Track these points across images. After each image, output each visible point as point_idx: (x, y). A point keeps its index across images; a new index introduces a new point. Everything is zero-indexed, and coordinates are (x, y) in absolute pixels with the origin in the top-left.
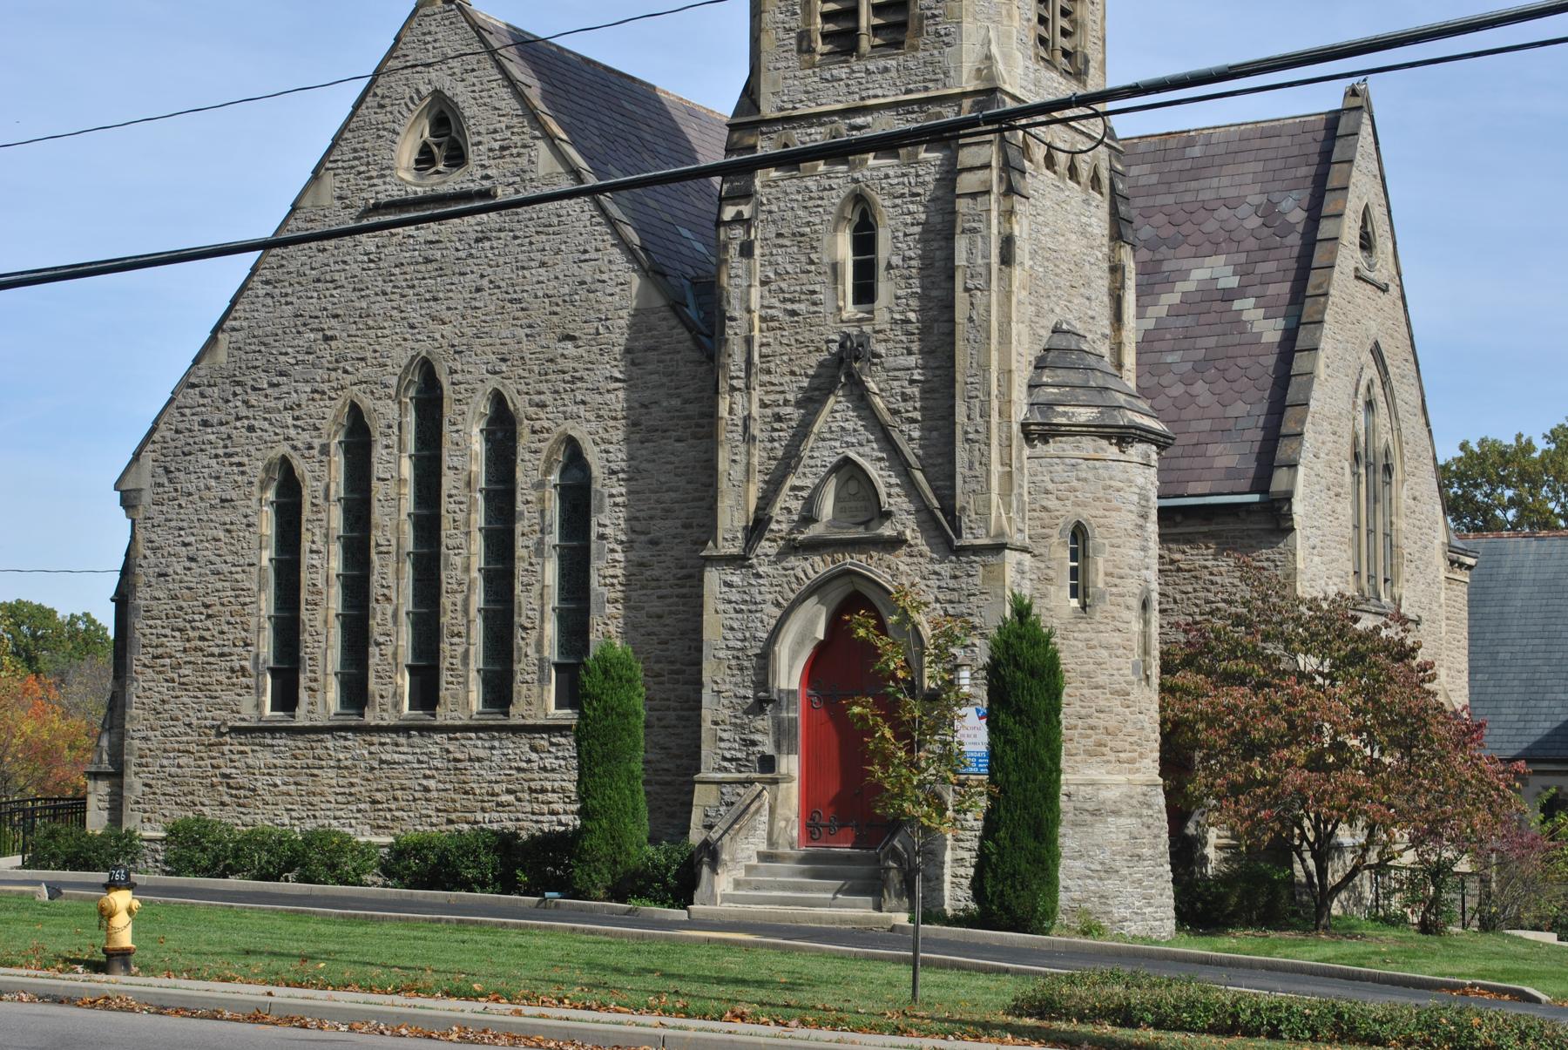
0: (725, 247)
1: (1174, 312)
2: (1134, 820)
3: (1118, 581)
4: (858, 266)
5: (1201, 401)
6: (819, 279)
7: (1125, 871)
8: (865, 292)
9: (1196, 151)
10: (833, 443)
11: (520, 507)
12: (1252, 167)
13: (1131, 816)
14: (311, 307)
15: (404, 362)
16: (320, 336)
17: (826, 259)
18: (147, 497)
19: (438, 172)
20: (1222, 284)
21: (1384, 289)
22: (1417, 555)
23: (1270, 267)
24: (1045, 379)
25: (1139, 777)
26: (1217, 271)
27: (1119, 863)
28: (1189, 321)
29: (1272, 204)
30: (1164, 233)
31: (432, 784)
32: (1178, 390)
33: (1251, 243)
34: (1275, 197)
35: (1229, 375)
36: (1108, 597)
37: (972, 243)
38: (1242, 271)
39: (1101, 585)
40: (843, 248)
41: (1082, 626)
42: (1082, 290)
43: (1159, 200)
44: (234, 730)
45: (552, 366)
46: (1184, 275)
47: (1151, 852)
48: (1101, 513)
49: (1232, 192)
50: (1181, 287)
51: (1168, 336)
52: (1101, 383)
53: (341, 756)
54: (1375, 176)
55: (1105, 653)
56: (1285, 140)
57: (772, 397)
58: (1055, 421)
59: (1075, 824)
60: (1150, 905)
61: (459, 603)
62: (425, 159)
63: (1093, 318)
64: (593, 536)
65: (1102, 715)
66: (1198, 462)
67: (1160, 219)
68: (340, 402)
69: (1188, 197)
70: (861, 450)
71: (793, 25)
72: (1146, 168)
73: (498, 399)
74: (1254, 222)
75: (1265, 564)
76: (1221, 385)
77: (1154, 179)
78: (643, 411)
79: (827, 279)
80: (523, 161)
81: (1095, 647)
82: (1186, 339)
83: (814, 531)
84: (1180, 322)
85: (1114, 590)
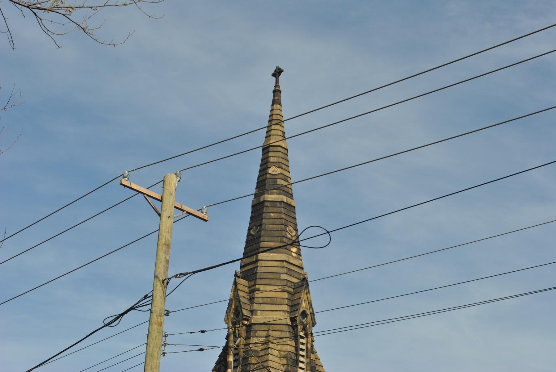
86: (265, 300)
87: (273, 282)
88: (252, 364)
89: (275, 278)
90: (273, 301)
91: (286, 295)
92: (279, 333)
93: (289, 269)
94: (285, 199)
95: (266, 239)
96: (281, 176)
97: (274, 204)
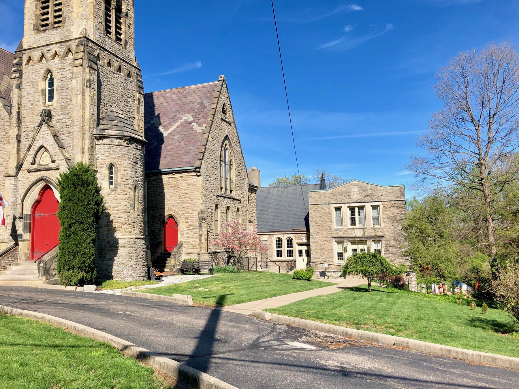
1: (178, 127)
2: (129, 249)
4: (50, 91)
6: (39, 94)
7: (127, 263)
8: (51, 98)
9: (187, 91)
10: (39, 141)
17: (40, 89)
20: (189, 120)
21: (230, 124)
23: (201, 116)
24: (104, 123)
25: (134, 236)
26: (189, 117)
27: (124, 261)
28: (181, 128)
29: (202, 102)
33: (197, 111)
35: (189, 140)
36: (122, 185)
38: (194, 117)
39: (119, 181)
40: (44, 85)
41: (112, 193)
42: (124, 103)
43: (177, 102)
46: (181, 118)
47: (136, 257)
48: (120, 160)
49: (194, 100)
50: (180, 121)
54: (227, 98)
55: (121, 201)
56: (206, 88)
57: (25, 129)
58: (104, 134)
59: (109, 250)
60: (134, 273)
63: (129, 112)
65: (120, 219)
67: (177, 106)
69: (184, 101)
70: (47, 143)
71: (32, 22)
72: (175, 95)
74: (198, 106)
77: (177, 98)
79: (40, 94)
81: (117, 199)
83: (35, 167)
84: (179, 129)
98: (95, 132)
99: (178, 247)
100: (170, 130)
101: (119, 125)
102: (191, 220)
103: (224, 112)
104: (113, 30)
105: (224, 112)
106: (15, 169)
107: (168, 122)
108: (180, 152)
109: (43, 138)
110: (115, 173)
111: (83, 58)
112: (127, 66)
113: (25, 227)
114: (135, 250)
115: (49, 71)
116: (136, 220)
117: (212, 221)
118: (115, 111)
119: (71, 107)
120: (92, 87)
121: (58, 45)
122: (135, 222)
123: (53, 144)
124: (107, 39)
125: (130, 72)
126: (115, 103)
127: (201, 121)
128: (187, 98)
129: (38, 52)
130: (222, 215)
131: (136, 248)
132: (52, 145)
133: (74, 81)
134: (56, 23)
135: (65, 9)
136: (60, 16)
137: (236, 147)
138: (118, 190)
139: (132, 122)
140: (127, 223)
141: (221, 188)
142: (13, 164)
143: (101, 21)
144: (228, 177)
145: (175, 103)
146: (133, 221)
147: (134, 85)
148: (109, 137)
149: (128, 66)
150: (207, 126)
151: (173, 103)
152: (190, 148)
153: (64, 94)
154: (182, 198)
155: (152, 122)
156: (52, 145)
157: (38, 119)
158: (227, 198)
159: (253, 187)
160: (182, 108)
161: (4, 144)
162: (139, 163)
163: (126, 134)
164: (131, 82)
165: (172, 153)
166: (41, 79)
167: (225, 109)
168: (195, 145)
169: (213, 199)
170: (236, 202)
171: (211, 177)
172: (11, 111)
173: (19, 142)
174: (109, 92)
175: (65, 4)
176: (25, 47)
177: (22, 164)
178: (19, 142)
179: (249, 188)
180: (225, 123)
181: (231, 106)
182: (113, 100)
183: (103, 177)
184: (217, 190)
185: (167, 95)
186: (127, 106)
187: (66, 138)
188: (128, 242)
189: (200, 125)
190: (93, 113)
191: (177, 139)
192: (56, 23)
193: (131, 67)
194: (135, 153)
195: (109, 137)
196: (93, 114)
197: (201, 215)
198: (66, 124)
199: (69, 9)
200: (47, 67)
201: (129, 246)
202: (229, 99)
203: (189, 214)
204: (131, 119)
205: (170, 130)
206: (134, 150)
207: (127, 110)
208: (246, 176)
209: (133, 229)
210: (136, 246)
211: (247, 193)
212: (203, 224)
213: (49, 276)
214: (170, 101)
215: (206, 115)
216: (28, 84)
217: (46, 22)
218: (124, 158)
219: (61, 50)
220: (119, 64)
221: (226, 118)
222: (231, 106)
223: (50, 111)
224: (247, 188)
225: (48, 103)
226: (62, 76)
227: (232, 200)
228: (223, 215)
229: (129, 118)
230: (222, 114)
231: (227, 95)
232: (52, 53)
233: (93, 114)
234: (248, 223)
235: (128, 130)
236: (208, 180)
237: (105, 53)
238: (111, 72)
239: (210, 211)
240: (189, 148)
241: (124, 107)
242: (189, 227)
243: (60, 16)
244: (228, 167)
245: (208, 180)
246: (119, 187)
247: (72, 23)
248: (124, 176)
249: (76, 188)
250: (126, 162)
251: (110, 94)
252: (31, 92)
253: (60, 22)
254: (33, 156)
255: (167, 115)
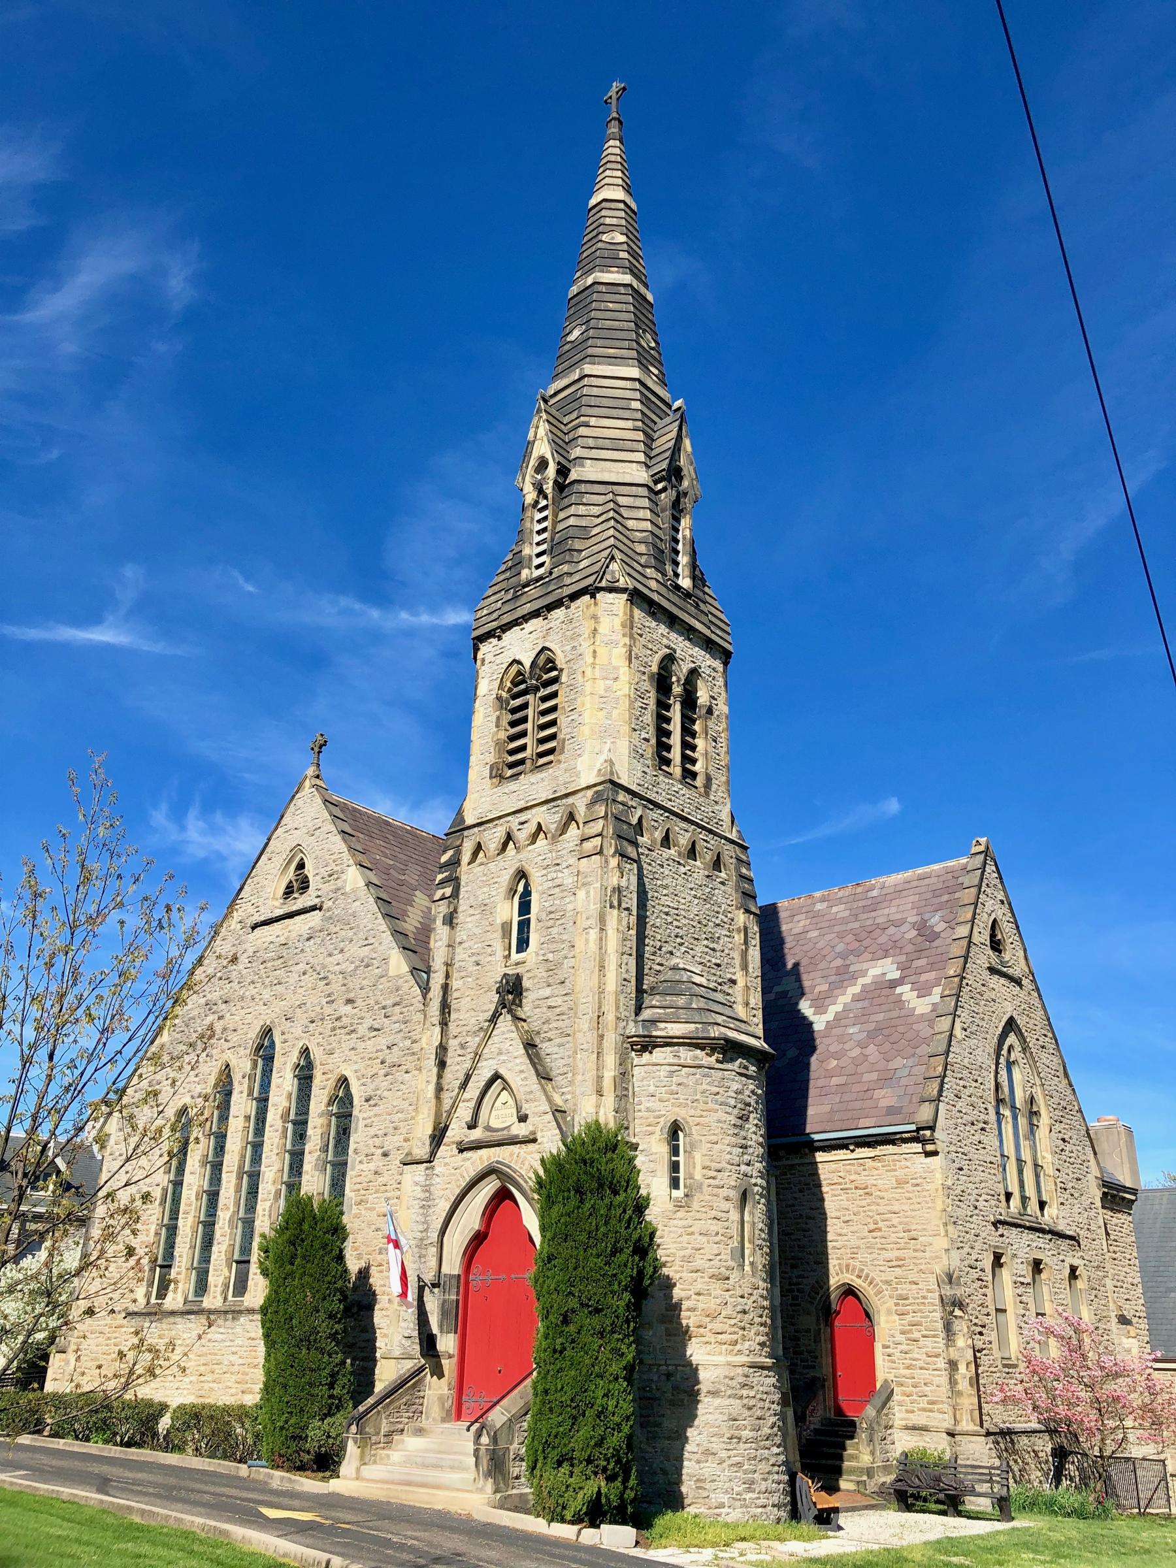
0: (435, 920)
1: (856, 999)
2: (732, 1401)
3: (714, 1174)
4: (520, 924)
5: (871, 1059)
7: (724, 1454)
8: (523, 944)
9: (875, 893)
11: (310, 1132)
12: (911, 899)
13: (729, 1397)
14: (214, 996)
15: (258, 1030)
16: (216, 1016)
17: (499, 921)
18: (112, 1141)
19: (295, 898)
20: (888, 977)
21: (1018, 982)
22: (1071, 1184)
23: (923, 962)
24: (654, 1002)
25: (743, 1359)
27: (717, 1445)
28: (866, 1003)
30: (851, 947)
31: (233, 1358)
32: (856, 1052)
33: (910, 948)
34: (926, 917)
35: (892, 1039)
36: (705, 1188)
37: (588, 893)
38: (902, 967)
39: (698, 1176)
40: (509, 911)
41: (679, 1215)
42: (706, 942)
44: (129, 1314)
45: (338, 1024)
46: (864, 973)
47: (751, 1434)
48: (699, 1113)
49: (899, 916)
50: (861, 981)
51: (852, 1015)
52: (702, 1005)
53: (185, 1336)
54: (1002, 902)
55: (705, 1239)
57: (459, 1030)
58: (654, 1033)
59: (673, 1403)
60: (750, 1490)
61: (267, 1209)
62: (289, 892)
63: (718, 965)
64: (351, 1151)
65: (701, 1297)
66: (868, 1104)
67: (850, 938)
68: (220, 1063)
69: (869, 922)
70: (510, 1065)
73: (305, 1052)
74: (914, 933)
75: (918, 1181)
76: (887, 1046)
77: (847, 913)
78: (388, 1051)
79: (499, 934)
80: (339, 883)
81: (692, 1233)
82: (862, 1017)
83: (477, 1134)
84: (860, 1005)
85: (711, 1181)
86: (600, 443)
87: (615, 413)
88: (576, 550)
89: (617, 408)
90: (617, 445)
91: (640, 436)
92: (631, 499)
93: (646, 397)
94: (635, 284)
95: (599, 342)
96: (625, 247)
97: (614, 289)
98: (632, 1029)
99: (877, 1401)
100: (833, 1010)
101: (694, 1006)
102: (916, 1307)
103: (996, 945)
104: (676, 754)
105: (996, 945)
106: (428, 1142)
107: (825, 987)
108: (867, 1077)
109: (500, 1053)
110: (685, 1152)
111: (605, 833)
112: (712, 842)
113: (444, 1313)
114: (750, 1409)
115: (521, 875)
116: (750, 1302)
117: (985, 1311)
118: (681, 966)
119: (572, 962)
120: (624, 905)
121: (545, 808)
122: (744, 1312)
123: (523, 1068)
124: (661, 778)
125: (719, 854)
126: (681, 944)
127: (924, 977)
128: (879, 912)
129: (499, 829)
130: (1019, 1291)
131: (752, 1402)
132: (522, 1072)
133: (581, 894)
134: (541, 755)
135: (563, 721)
136: (553, 737)
137: (1043, 1055)
138: (695, 1205)
139: (728, 994)
140: (724, 1313)
141: (1008, 1196)
142: (426, 1129)
143: (647, 736)
144: (1026, 1155)
145: (844, 927)
146: (739, 1308)
147: (730, 889)
148: (668, 1042)
149: (713, 842)
150: (947, 993)
151: (837, 929)
152: (898, 1062)
153: (554, 931)
154: (880, 1229)
155: (777, 989)
156: (522, 1072)
157: (491, 1000)
158: (1031, 1229)
159: (1119, 1191)
160: (865, 943)
161: (407, 1072)
162: (751, 1119)
163: (715, 1032)
164: (722, 883)
165: (841, 1080)
166: (502, 896)
167: (999, 937)
168: (913, 1055)
169: (983, 1235)
170: (1064, 1244)
171: (970, 1156)
172: (428, 984)
173: (442, 1064)
174: (667, 914)
175: (563, 707)
176: (469, 821)
177: (446, 1128)
178: (442, 1064)
179: (1104, 1193)
180: (1003, 981)
181: (1018, 927)
182: (677, 936)
183: (652, 1165)
184: (993, 1203)
185: (819, 906)
186: (713, 950)
187: (555, 1049)
188: (726, 1377)
189: (923, 991)
190: (625, 976)
191: (855, 1038)
192: (541, 755)
193: (723, 841)
194: (740, 1087)
195: (668, 1042)
196: (625, 980)
197: (948, 1291)
198: (558, 1010)
199: (572, 718)
200: (518, 865)
201: (729, 1392)
202: (1010, 904)
203: (908, 1286)
204: (725, 988)
205: (833, 1010)
206: (738, 1078)
207: (714, 961)
208: (1089, 1150)
209: (741, 1332)
210: (752, 1394)
211: (1101, 1211)
212: (957, 1322)
213: (504, 1479)
214: (827, 924)
215: (938, 958)
216: (472, 911)
217: (520, 756)
218: (711, 1105)
219: (550, 818)
220: (690, 838)
221: (1003, 963)
222: (1018, 927)
223: (519, 978)
224: (1097, 1194)
225: (515, 957)
226: (550, 884)
227: (1049, 1236)
228: (1021, 1290)
229: (720, 984)
230: (991, 952)
231: (1000, 896)
232: (531, 827)
233: (625, 980)
234: (1114, 1324)
235: (720, 1019)
236: (961, 1169)
237: (656, 814)
238: (671, 862)
239: (976, 1276)
240: (892, 1065)
241: (707, 953)
242: (910, 1332)
243: (553, 737)
244: (1022, 1121)
245: (961, 1169)
246: (697, 1197)
247: (579, 752)
248: (712, 1161)
249: (582, 1201)
250: (716, 1116)
251: (669, 919)
252: (477, 931)
253: (551, 751)
254: (472, 1104)
255: (819, 967)
